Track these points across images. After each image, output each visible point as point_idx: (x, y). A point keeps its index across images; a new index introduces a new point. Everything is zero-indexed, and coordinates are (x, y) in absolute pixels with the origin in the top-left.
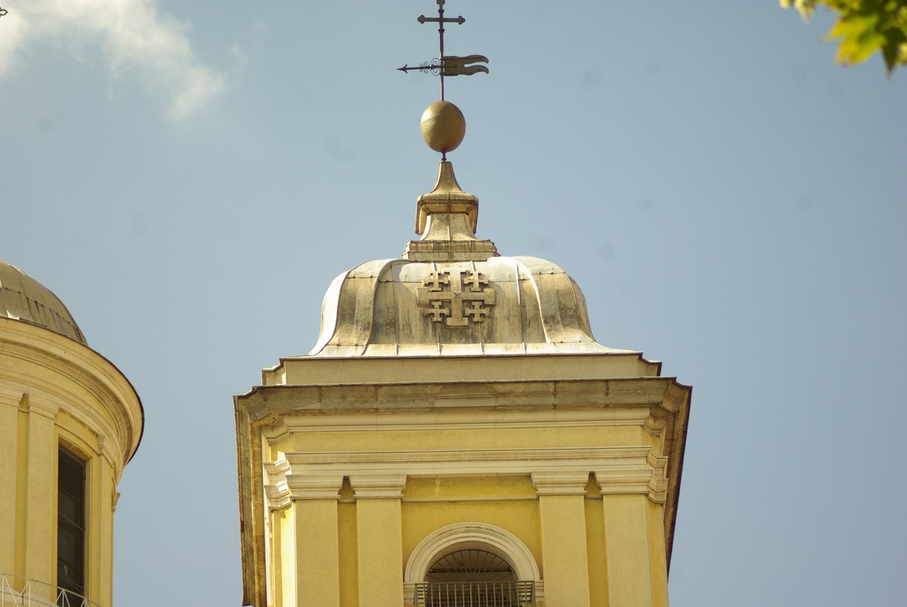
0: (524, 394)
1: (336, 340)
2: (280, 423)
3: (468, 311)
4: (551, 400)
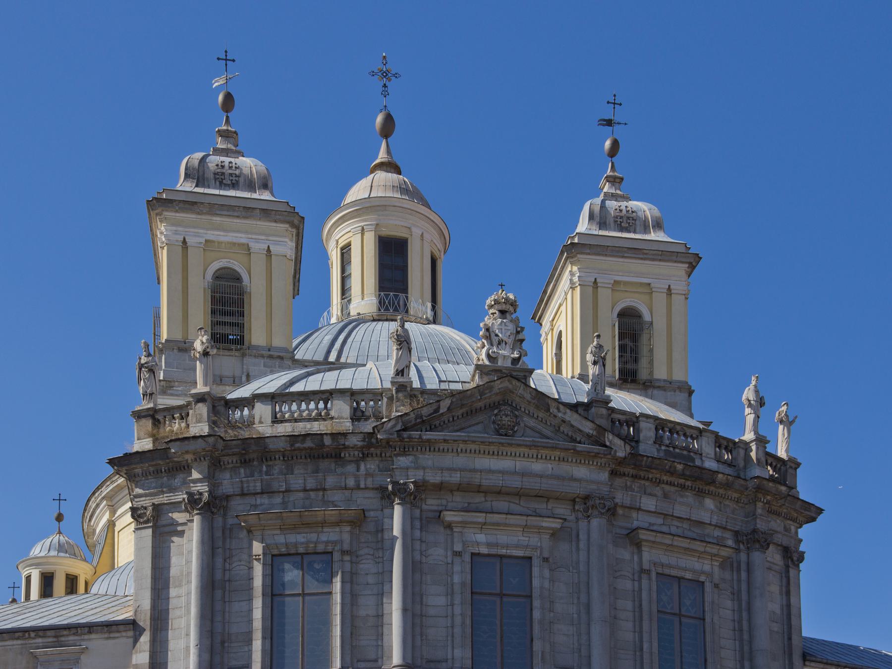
0: (653, 255)
1: (589, 227)
2: (575, 256)
3: (628, 221)
4: (660, 258)
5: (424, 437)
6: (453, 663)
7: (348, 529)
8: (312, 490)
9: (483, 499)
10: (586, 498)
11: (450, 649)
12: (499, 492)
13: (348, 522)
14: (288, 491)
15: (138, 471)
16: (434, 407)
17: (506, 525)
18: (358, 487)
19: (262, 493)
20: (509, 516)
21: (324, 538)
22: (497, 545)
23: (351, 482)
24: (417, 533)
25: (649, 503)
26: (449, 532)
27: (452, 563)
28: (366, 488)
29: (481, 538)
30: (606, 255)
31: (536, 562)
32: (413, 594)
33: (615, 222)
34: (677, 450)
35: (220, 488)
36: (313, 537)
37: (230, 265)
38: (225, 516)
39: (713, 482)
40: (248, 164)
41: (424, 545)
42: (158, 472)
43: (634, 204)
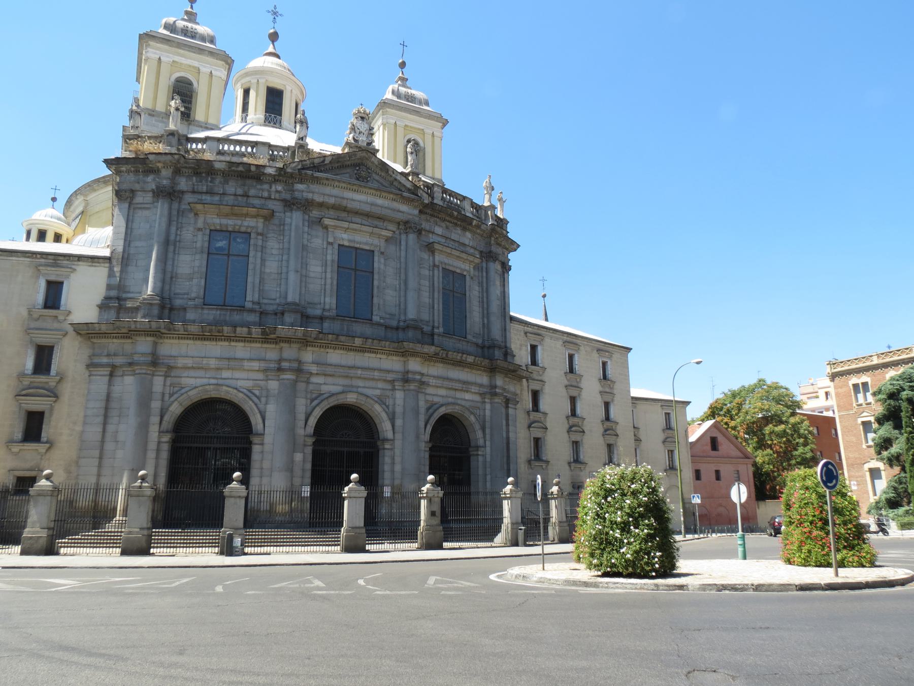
6: (324, 306)
7: (262, 220)
8: (240, 195)
9: (347, 215)
10: (406, 223)
11: (322, 297)
12: (357, 213)
13: (262, 216)
14: (224, 194)
15: (124, 169)
17: (360, 231)
18: (269, 198)
19: (207, 193)
20: (363, 226)
21: (246, 224)
22: (354, 241)
24: (306, 229)
25: (439, 230)
26: (325, 231)
27: (327, 248)
28: (275, 199)
29: (345, 236)
30: (401, 111)
31: (376, 253)
32: (302, 263)
33: (405, 97)
35: (179, 186)
36: (239, 222)
37: (186, 76)
38: (180, 202)
39: (471, 224)
40: (201, 29)
41: (310, 237)
42: (137, 171)
43: (413, 92)
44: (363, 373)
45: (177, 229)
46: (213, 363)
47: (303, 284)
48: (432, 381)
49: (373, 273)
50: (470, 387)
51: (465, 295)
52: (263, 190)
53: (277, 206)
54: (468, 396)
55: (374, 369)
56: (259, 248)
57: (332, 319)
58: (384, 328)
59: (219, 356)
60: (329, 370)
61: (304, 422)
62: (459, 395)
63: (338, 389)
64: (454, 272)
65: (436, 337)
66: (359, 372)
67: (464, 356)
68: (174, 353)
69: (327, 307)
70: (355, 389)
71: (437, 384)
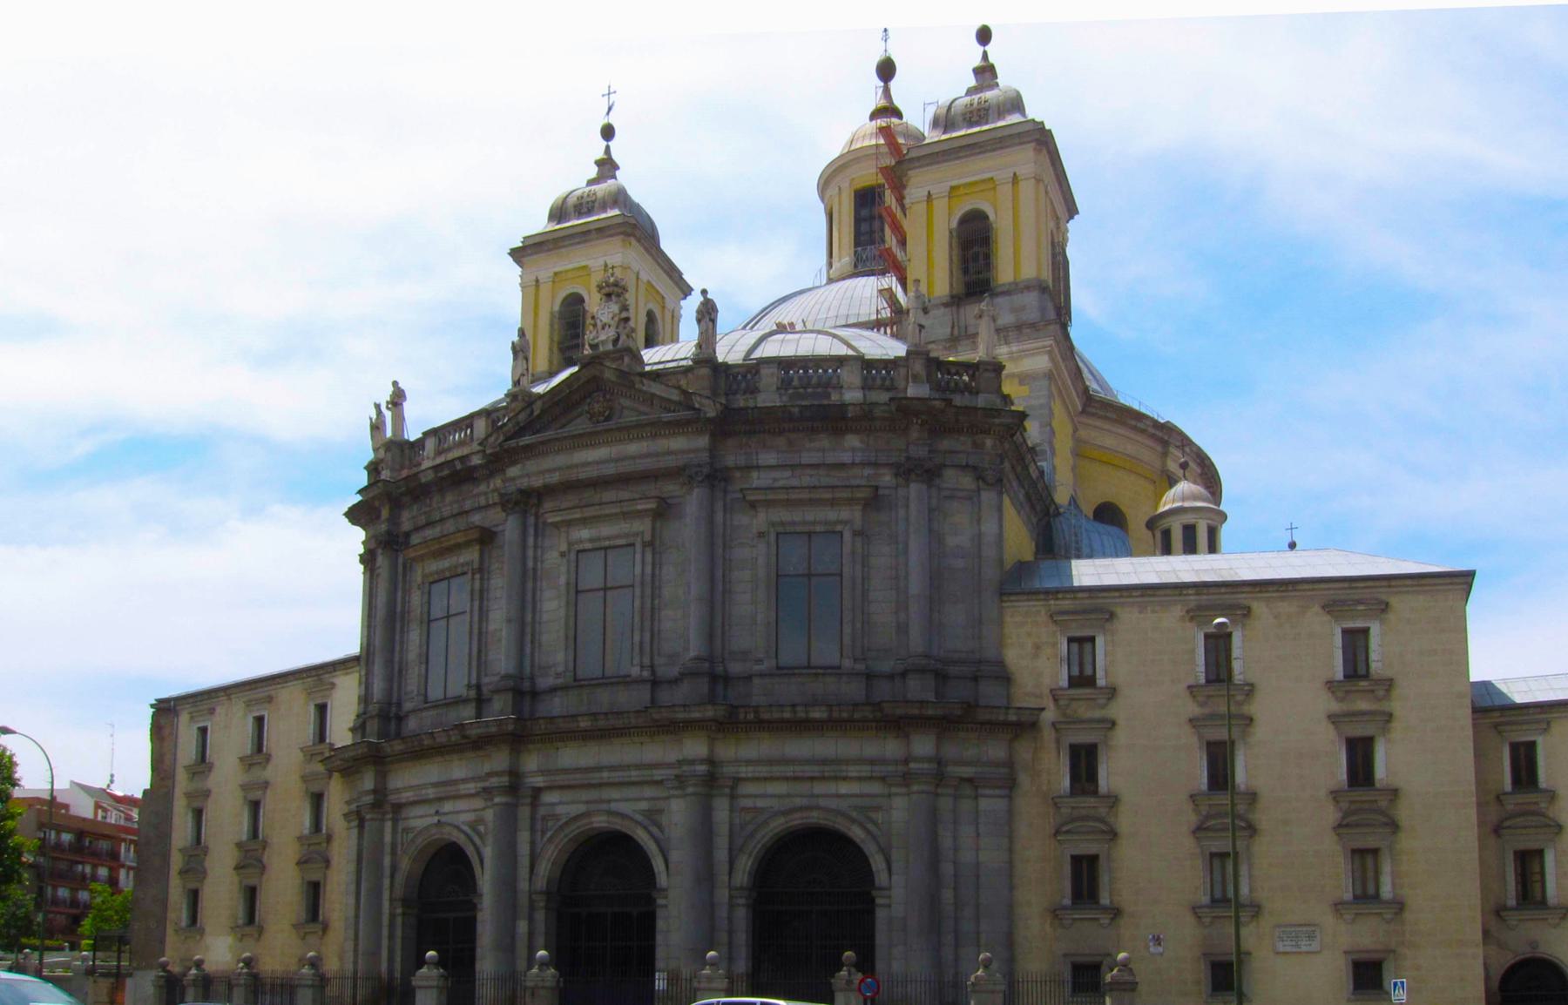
5: (521, 444)
16: (528, 411)
18: (487, 507)
22: (598, 539)
23: (483, 501)
24: (531, 541)
25: (768, 458)
29: (585, 533)
34: (810, 390)
44: (614, 774)
45: (404, 591)
46: (431, 793)
47: (528, 638)
48: (745, 771)
49: (633, 586)
50: (844, 768)
51: (841, 575)
52: (478, 495)
53: (494, 517)
54: (844, 788)
55: (628, 767)
56: (477, 596)
57: (565, 688)
58: (648, 686)
59: (435, 779)
60: (560, 779)
61: (528, 870)
62: (819, 788)
63: (582, 808)
64: (810, 534)
65: (756, 681)
66: (605, 774)
67: (799, 708)
68: (399, 784)
69: (560, 669)
70: (604, 806)
71: (757, 775)
